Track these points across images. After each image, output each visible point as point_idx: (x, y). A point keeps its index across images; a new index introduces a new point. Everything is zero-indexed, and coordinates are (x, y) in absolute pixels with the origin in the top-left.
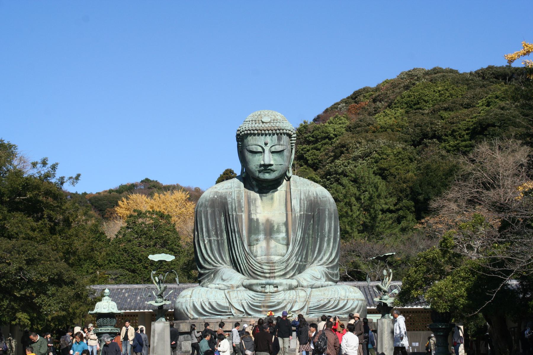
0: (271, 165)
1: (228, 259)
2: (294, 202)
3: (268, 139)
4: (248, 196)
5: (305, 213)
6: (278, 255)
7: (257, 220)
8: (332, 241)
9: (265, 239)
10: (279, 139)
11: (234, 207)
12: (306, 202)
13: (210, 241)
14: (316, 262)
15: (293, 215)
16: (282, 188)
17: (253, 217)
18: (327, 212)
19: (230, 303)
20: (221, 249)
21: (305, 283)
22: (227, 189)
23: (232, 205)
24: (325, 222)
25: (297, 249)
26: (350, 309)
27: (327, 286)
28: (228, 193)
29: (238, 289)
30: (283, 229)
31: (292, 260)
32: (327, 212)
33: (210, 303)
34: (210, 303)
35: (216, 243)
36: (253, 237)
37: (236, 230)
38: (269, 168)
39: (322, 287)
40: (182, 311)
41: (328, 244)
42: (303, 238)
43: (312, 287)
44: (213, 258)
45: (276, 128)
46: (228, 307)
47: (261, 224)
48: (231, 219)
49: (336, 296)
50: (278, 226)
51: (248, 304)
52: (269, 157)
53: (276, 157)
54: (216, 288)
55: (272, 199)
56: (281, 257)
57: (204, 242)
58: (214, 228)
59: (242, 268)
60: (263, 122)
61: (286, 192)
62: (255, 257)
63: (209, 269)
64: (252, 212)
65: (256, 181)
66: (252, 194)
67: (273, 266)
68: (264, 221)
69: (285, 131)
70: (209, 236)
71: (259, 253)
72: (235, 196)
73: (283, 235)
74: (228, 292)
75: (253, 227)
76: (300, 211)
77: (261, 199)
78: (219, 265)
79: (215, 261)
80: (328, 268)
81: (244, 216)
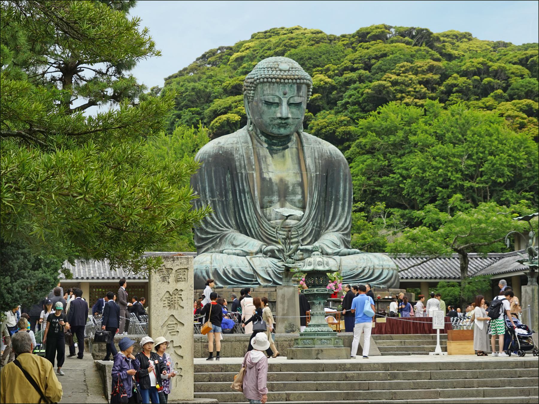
1: (233, 222)
2: (309, 161)
4: (257, 152)
6: (294, 219)
7: (270, 179)
8: (347, 204)
9: (279, 201)
10: (299, 89)
11: (243, 165)
12: (320, 161)
13: (213, 202)
14: (331, 228)
15: (309, 175)
16: (292, 145)
17: (265, 176)
18: (342, 174)
19: (255, 271)
20: (226, 211)
21: (330, 251)
22: (232, 144)
23: (240, 162)
24: (339, 184)
25: (313, 213)
26: (387, 278)
27: (355, 253)
28: (235, 147)
29: (257, 255)
30: (299, 190)
31: (309, 225)
33: (233, 271)
34: (233, 271)
36: (266, 199)
37: (246, 189)
38: (286, 121)
39: (349, 254)
40: (202, 278)
41: (343, 209)
42: (319, 201)
43: (337, 254)
44: (217, 221)
45: (296, 77)
46: (253, 275)
47: (274, 184)
48: (240, 178)
49: (369, 264)
50: (294, 187)
51: (274, 273)
53: (294, 110)
54: (234, 254)
55: (284, 156)
56: (297, 221)
57: (207, 202)
58: (218, 187)
59: (254, 233)
60: (281, 70)
61: (297, 149)
62: (269, 220)
63: (213, 234)
64: (264, 170)
65: (265, 137)
66: (261, 151)
69: (305, 81)
70: (213, 196)
71: (273, 216)
72: (242, 151)
73: (299, 197)
74: (251, 258)
75: (267, 187)
77: (272, 156)
78: (225, 229)
79: (221, 225)
80: (343, 234)
81: (256, 175)
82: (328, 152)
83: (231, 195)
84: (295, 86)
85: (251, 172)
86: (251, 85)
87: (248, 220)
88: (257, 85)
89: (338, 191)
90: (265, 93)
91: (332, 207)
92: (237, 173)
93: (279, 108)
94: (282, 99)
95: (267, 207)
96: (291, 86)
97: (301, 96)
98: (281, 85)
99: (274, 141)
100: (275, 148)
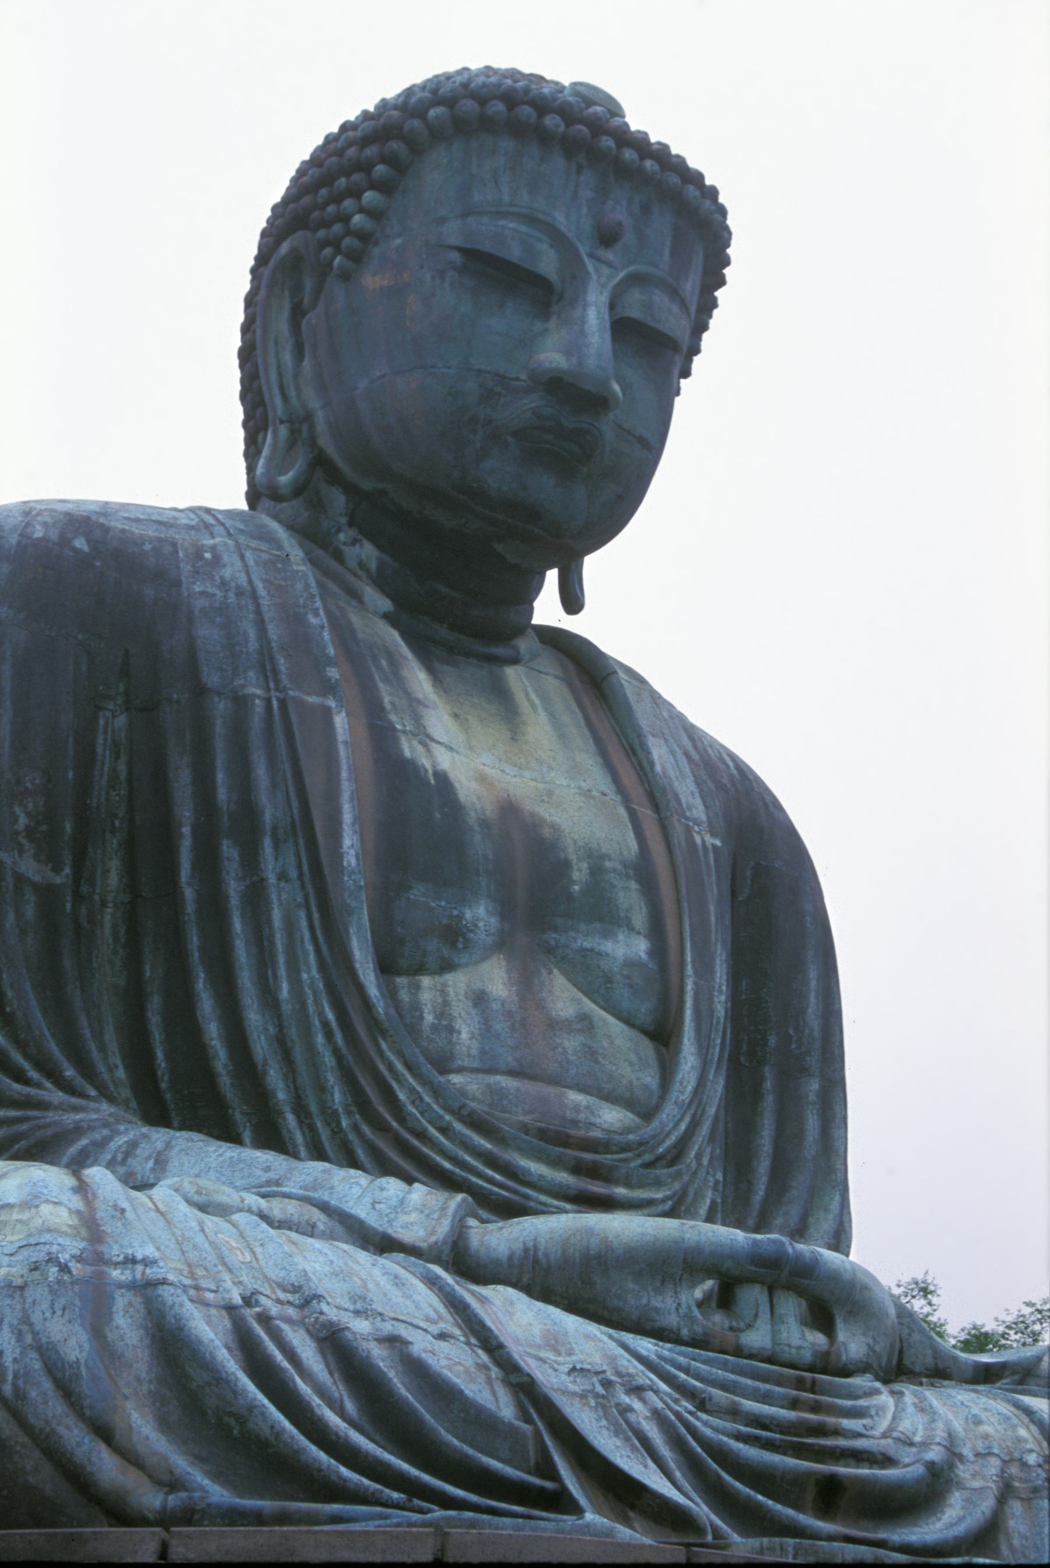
1: (117, 1071)
6: (612, 1098)
7: (443, 780)
11: (253, 645)
17: (407, 753)
19: (526, 1390)
20: (67, 963)
35: (30, 911)
37: (270, 810)
48: (219, 728)
50: (597, 871)
51: (678, 1444)
58: (32, 780)
64: (393, 718)
67: (594, 1172)
68: (490, 810)
77: (430, 670)
82: (731, 764)
83: (115, 865)
85: (312, 699)
86: (371, 151)
87: (261, 1046)
88: (416, 148)
90: (477, 197)
91: (769, 1102)
92: (200, 691)
93: (552, 324)
94: (590, 265)
95: (420, 969)
96: (646, 209)
98: (588, 178)
100: (443, 632)
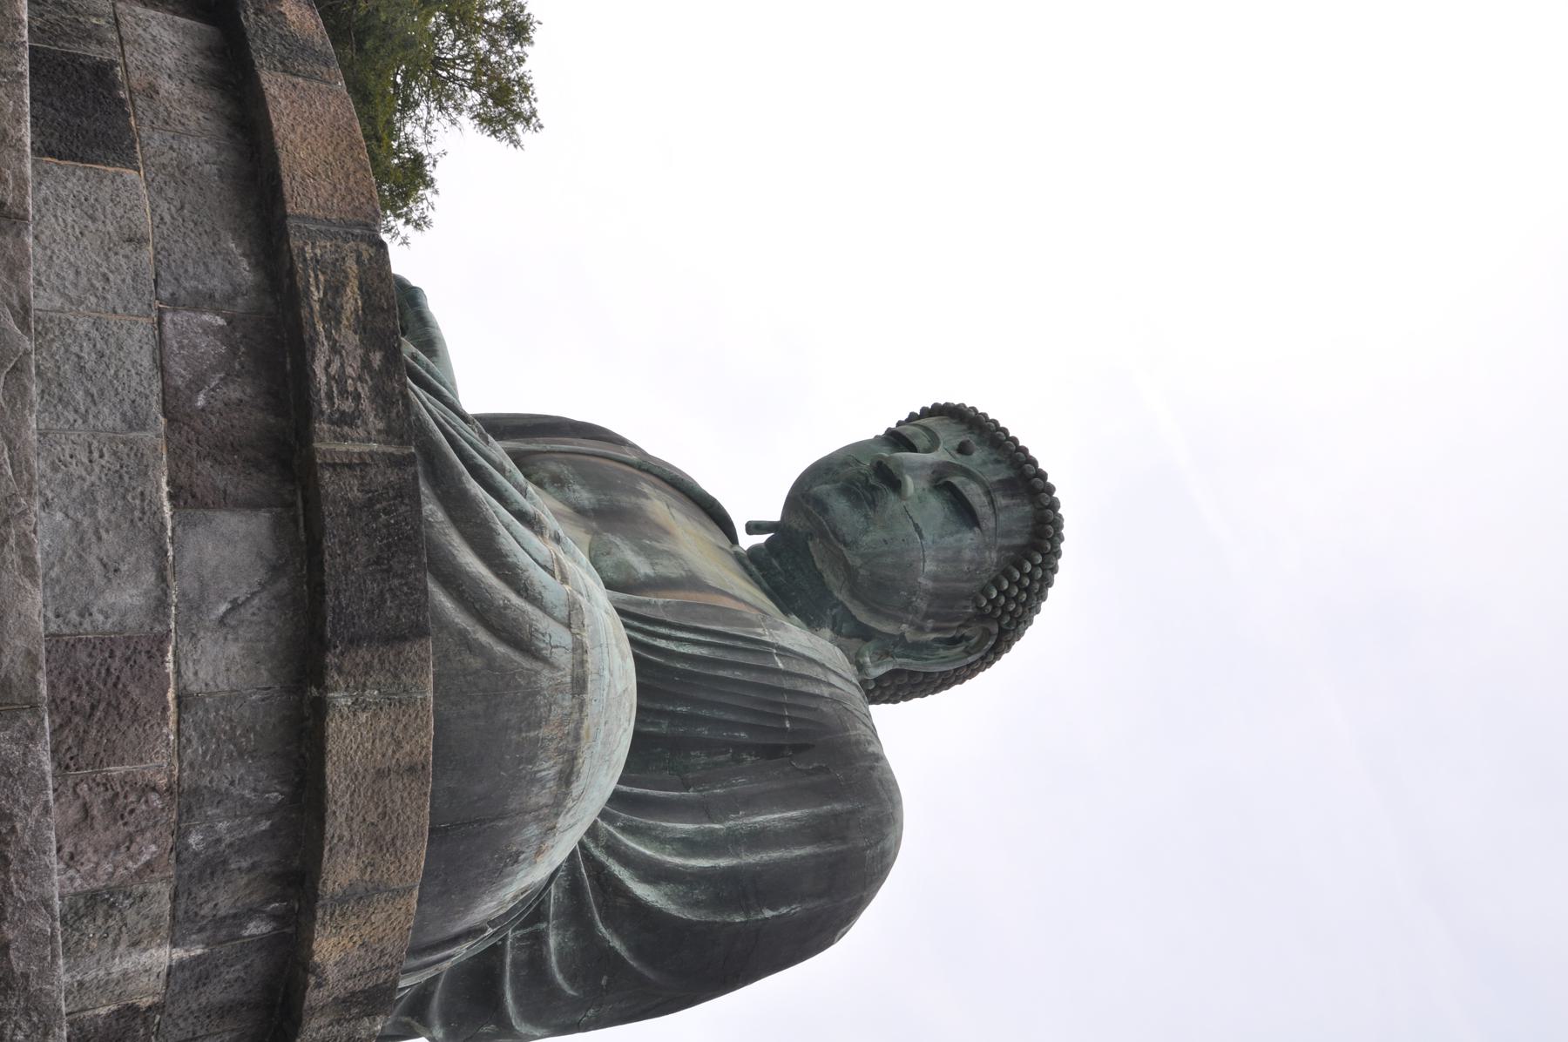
0: (896, 485)
3: (979, 454)
5: (787, 684)
8: (723, 862)
10: (1009, 487)
12: (826, 691)
18: (838, 807)
32: (838, 807)
50: (671, 555)
52: (923, 466)
73: (643, 568)
76: (784, 652)
84: (1004, 473)
89: (751, 803)
96: (997, 462)
97: (992, 502)
99: (775, 563)
